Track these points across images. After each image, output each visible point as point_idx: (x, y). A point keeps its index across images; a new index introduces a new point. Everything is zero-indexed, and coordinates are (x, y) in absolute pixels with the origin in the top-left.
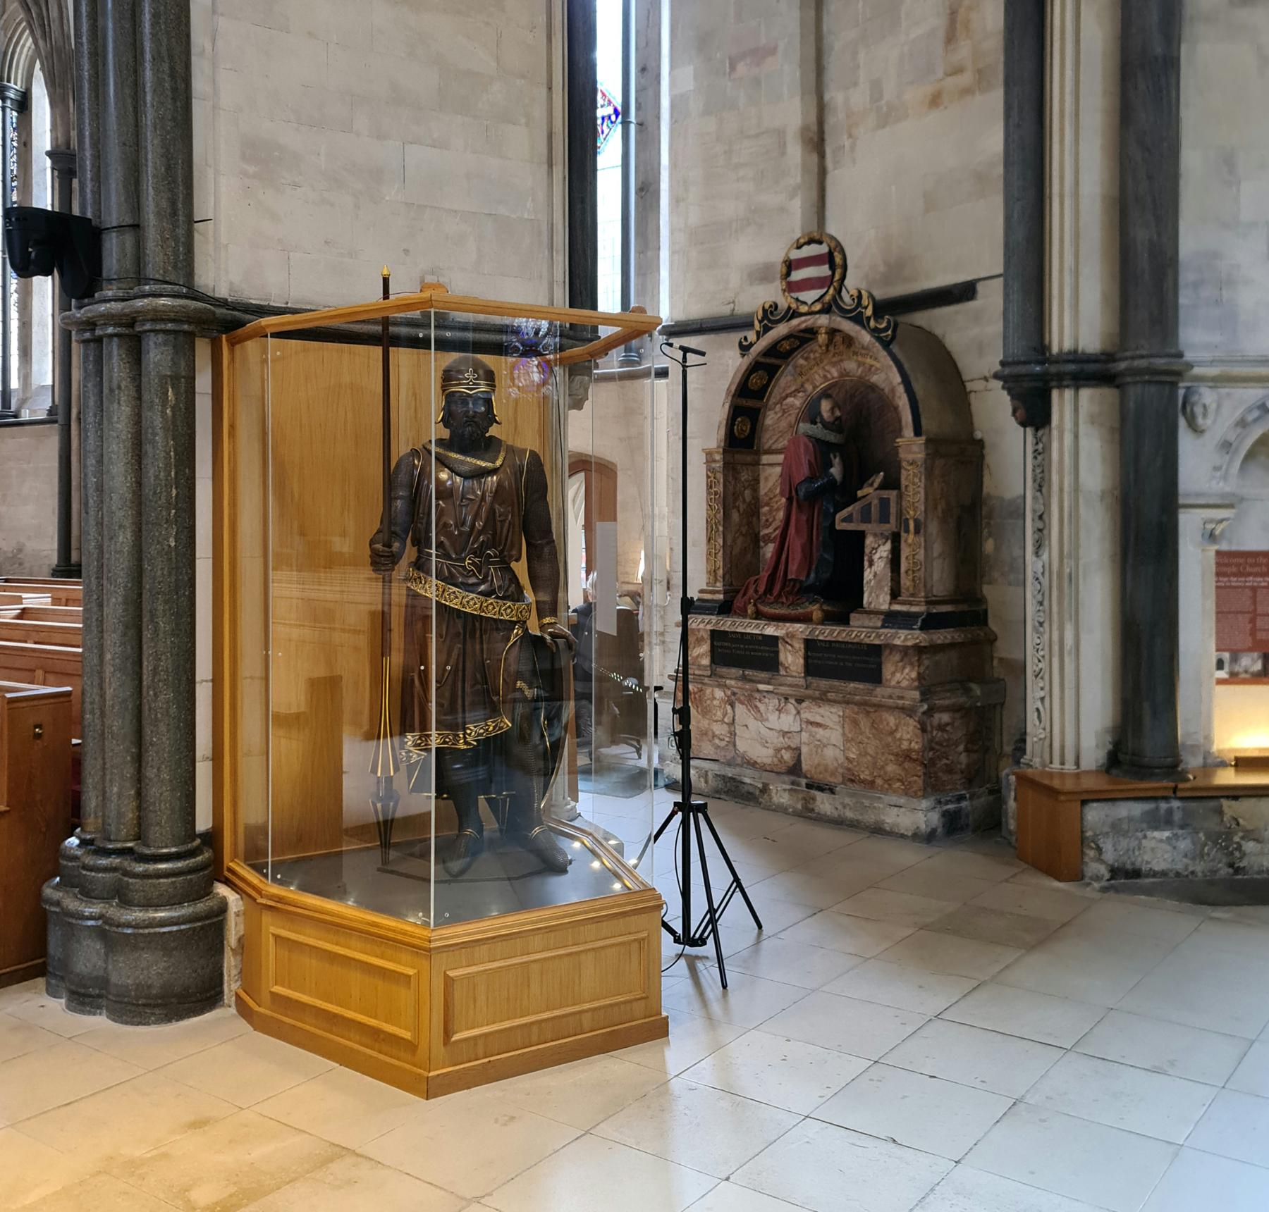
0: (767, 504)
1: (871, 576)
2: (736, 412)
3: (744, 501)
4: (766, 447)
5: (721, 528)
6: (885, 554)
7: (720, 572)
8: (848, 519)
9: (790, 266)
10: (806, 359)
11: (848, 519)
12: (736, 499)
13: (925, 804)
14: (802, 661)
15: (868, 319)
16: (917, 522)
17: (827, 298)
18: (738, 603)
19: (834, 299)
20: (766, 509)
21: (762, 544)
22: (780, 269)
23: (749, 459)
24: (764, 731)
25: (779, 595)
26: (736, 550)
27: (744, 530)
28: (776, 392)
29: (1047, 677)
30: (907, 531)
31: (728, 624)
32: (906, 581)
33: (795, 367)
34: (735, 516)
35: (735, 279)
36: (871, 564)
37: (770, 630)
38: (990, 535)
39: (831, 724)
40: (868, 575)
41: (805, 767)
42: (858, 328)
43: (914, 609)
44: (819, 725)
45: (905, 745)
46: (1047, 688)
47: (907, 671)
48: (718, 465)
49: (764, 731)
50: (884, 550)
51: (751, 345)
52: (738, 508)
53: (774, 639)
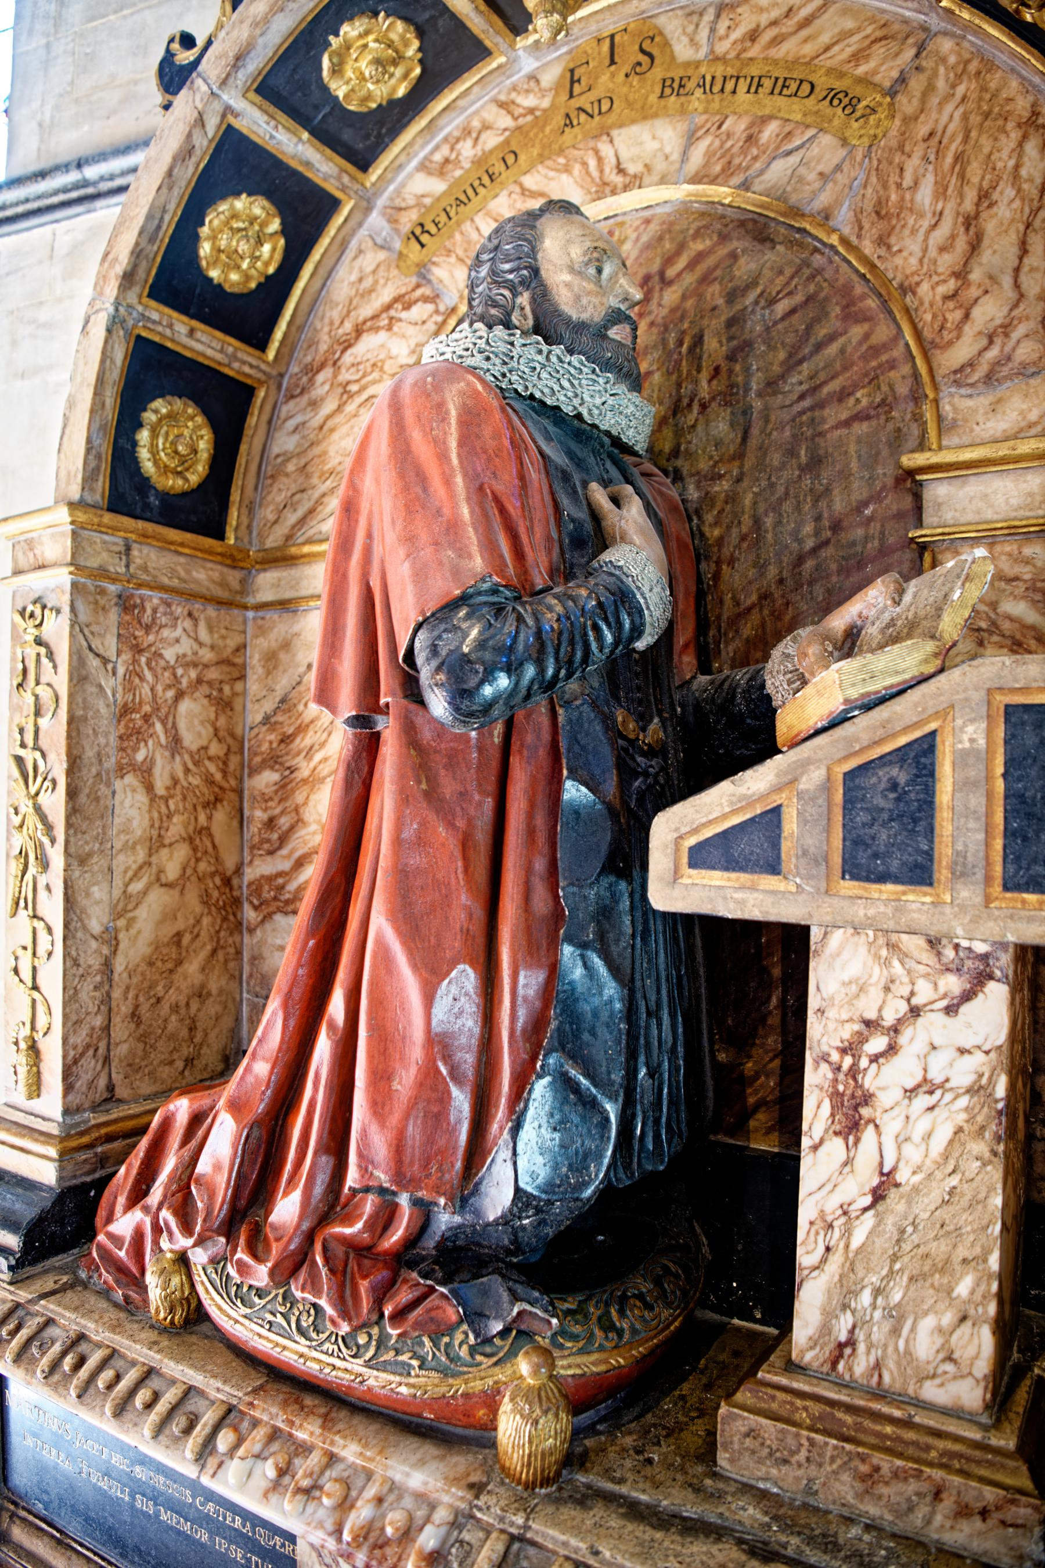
0: (273, 761)
1: (855, 1189)
3: (175, 743)
6: (964, 1073)
20: (267, 779)
21: (250, 915)
26: (132, 952)
34: (129, 807)
36: (853, 1115)
52: (145, 773)
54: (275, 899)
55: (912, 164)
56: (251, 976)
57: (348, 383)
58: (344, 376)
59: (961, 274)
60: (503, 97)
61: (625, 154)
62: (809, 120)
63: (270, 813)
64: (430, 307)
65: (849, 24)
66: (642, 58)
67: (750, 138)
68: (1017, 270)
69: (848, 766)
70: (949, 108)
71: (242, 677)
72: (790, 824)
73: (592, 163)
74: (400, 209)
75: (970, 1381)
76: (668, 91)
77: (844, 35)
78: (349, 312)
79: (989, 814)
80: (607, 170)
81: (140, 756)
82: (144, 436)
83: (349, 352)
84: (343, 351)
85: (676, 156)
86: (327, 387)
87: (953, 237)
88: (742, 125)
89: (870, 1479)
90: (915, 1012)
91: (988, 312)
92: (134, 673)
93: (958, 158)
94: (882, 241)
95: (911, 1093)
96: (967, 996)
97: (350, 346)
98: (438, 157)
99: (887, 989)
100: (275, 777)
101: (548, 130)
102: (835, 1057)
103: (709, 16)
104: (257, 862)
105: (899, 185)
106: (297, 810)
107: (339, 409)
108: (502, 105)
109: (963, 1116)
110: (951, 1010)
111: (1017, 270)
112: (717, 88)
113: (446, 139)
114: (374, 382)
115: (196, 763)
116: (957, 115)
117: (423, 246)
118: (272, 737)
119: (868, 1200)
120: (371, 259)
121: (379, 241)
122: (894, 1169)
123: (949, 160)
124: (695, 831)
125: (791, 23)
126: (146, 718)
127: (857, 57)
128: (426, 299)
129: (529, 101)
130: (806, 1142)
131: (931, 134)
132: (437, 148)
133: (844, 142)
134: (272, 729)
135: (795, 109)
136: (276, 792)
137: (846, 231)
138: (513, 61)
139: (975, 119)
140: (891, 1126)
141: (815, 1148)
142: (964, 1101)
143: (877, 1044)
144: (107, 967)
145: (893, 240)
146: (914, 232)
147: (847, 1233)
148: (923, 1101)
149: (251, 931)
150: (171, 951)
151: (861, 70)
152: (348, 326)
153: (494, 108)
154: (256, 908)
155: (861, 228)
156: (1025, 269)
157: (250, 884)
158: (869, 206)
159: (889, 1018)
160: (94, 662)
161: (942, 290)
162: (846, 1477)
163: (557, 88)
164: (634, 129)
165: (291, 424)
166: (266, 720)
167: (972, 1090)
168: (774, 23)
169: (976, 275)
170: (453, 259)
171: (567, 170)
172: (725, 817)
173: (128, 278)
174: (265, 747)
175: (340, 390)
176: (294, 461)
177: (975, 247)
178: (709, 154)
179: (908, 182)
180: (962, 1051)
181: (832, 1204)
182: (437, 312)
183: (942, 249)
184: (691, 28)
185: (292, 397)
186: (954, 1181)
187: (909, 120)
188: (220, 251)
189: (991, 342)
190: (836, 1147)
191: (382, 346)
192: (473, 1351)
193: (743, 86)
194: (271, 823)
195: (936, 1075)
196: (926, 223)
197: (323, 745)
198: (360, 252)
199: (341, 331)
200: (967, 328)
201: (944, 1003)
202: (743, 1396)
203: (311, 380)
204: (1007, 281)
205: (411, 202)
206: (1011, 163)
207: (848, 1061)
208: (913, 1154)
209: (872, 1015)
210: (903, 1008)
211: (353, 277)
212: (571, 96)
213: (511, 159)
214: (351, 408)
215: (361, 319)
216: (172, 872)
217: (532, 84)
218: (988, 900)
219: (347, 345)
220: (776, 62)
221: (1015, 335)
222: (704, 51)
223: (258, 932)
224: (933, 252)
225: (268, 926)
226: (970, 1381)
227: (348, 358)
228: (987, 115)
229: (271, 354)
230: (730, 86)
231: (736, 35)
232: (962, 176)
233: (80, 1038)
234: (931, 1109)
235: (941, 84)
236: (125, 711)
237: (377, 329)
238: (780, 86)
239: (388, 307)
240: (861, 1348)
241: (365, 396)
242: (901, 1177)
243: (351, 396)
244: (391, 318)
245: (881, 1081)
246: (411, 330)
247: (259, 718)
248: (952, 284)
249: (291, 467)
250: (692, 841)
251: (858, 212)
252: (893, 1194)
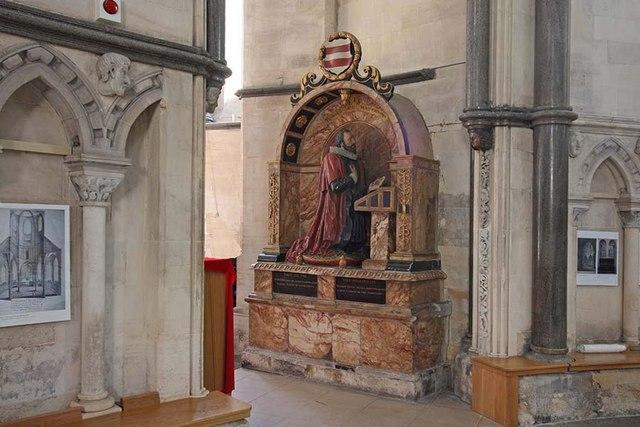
2: (288, 140)
7: (278, 236)
8: (363, 204)
9: (325, 52)
11: (363, 204)
13: (414, 378)
15: (376, 84)
16: (407, 207)
18: (290, 254)
19: (353, 72)
22: (318, 53)
23: (295, 168)
24: (308, 333)
25: (317, 250)
28: (310, 130)
29: (489, 300)
30: (401, 211)
31: (283, 267)
32: (400, 243)
34: (286, 202)
35: (283, 65)
37: (312, 272)
38: (443, 216)
39: (351, 328)
40: (373, 238)
41: (334, 355)
42: (369, 89)
43: (405, 259)
44: (344, 329)
45: (401, 342)
46: (489, 307)
48: (278, 172)
49: (308, 333)
50: (385, 223)
51: (299, 99)
53: (314, 278)
150: (291, 224)
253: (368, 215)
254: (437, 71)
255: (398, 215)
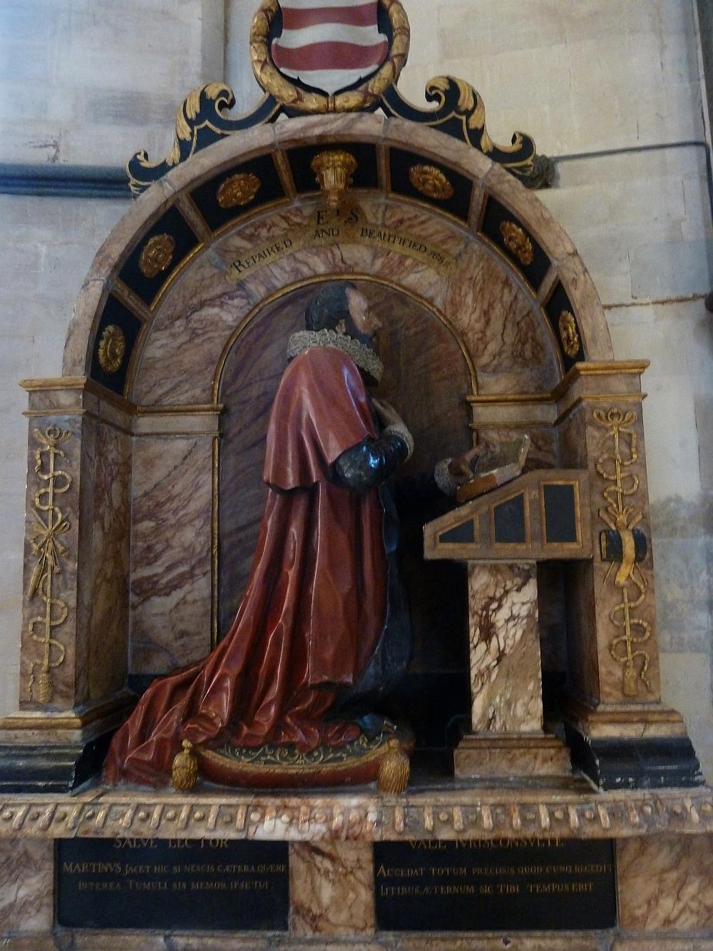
0: (150, 515)
1: (490, 660)
4: (148, 400)
5: (72, 566)
6: (524, 611)
10: (250, 238)
12: (99, 500)
14: (366, 896)
17: (376, 86)
20: (147, 525)
21: (133, 598)
23: (120, 418)
26: (98, 616)
27: (109, 571)
28: (173, 294)
31: (123, 812)
33: (223, 252)
34: (97, 538)
35: (60, 109)
36: (488, 632)
37: (271, 827)
40: (480, 657)
47: (691, 889)
51: (163, 169)
52: (102, 519)
53: (277, 851)
54: (152, 588)
55: (465, 288)
56: (133, 632)
57: (196, 329)
58: (193, 325)
59: (483, 332)
60: (283, 214)
61: (344, 254)
62: (424, 261)
63: (148, 543)
64: (245, 301)
65: (439, 227)
66: (351, 216)
67: (401, 262)
68: (503, 334)
69: (495, 505)
70: (477, 270)
71: (130, 472)
72: (477, 525)
73: (330, 255)
74: (226, 251)
75: (536, 720)
76: (364, 234)
77: (437, 232)
78: (195, 295)
79: (541, 520)
80: (337, 260)
81: (101, 511)
82: (102, 343)
83: (196, 313)
84: (194, 312)
85: (369, 261)
86: (182, 329)
87: (480, 317)
88: (397, 257)
89: (512, 761)
90: (506, 592)
91: (493, 347)
92: (99, 467)
93: (481, 289)
94: (454, 314)
95: (507, 621)
96: (524, 584)
97: (197, 311)
98: (248, 232)
99: (496, 585)
100: (152, 524)
101: (307, 235)
102: (480, 612)
103: (382, 208)
104: (138, 570)
105: (460, 295)
106: (167, 541)
107: (190, 340)
108: (283, 217)
109: (525, 627)
110: (519, 590)
111: (503, 334)
112: (386, 239)
113: (252, 225)
114: (212, 331)
115: (117, 516)
116: (481, 273)
117: (240, 271)
118: (150, 503)
119: (495, 662)
120: (208, 272)
121: (213, 263)
122: (504, 649)
123: (478, 289)
124: (442, 529)
125: (415, 222)
126: (103, 490)
127: (443, 242)
128: (242, 297)
129: (297, 220)
130: (471, 646)
131: (471, 278)
132: (247, 227)
133: (438, 273)
134: (150, 499)
135: (419, 256)
136: (153, 532)
137: (440, 307)
138: (291, 202)
139: (486, 277)
140: (502, 635)
141: (475, 647)
142: (525, 621)
143: (494, 606)
144: (89, 623)
145: (458, 314)
146: (466, 313)
147: (489, 677)
148: (511, 624)
149: (134, 607)
151: (445, 247)
152: (195, 301)
153: (278, 217)
154: (137, 595)
155: (445, 308)
156: (505, 334)
157: (133, 583)
158: (448, 300)
159: (498, 595)
160: (88, 460)
161: (476, 336)
162: (504, 762)
163: (310, 217)
164: (350, 246)
165: (158, 343)
166: (146, 494)
167: (528, 616)
168: (410, 219)
169: (488, 333)
170: (258, 281)
171: (317, 254)
172: (451, 525)
173: (116, 266)
174: (145, 509)
175: (191, 331)
176: (161, 362)
177: (488, 323)
178: (383, 266)
179: (463, 293)
180: (523, 604)
181: (483, 666)
182: (249, 304)
183: (476, 321)
184: (374, 211)
185: (159, 330)
186: (525, 649)
187: (463, 271)
188: (149, 257)
189: (494, 358)
190: (483, 646)
191: (217, 314)
192: (368, 744)
193: (397, 241)
194: (149, 549)
195: (515, 612)
196: (470, 311)
197: (184, 507)
198: (201, 266)
199: (191, 302)
200: (486, 352)
201: (515, 588)
202: (461, 744)
203: (172, 324)
204: (499, 337)
205: (233, 249)
206: (500, 295)
207: (484, 613)
208: (510, 642)
209: (491, 594)
210: (502, 591)
211: (198, 278)
212: (319, 223)
213: (288, 243)
214: (198, 341)
215: (203, 299)
216: (109, 576)
217: (298, 212)
218: (542, 546)
219: (195, 310)
220: (411, 235)
221: (504, 356)
222: (379, 223)
223: (140, 607)
224: (473, 321)
225: (147, 604)
226: (536, 720)
227: (195, 316)
228: (491, 276)
229: (152, 308)
230: (392, 239)
231: (394, 219)
232: (483, 296)
233: (80, 664)
234: (514, 625)
235: (475, 261)
236: (97, 486)
237: (214, 306)
238: (413, 245)
239: (220, 296)
240: (498, 718)
241: (206, 337)
242: (507, 651)
243: (198, 335)
244: (222, 303)
245: (497, 618)
246: (233, 310)
247: (141, 493)
248: (480, 335)
249: (158, 365)
250: (441, 533)
251: (444, 301)
252: (504, 659)
253: (456, 574)
254: (561, 168)
255: (601, 568)
